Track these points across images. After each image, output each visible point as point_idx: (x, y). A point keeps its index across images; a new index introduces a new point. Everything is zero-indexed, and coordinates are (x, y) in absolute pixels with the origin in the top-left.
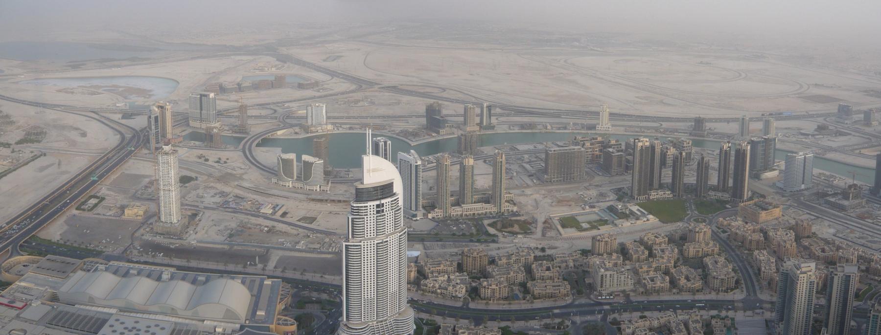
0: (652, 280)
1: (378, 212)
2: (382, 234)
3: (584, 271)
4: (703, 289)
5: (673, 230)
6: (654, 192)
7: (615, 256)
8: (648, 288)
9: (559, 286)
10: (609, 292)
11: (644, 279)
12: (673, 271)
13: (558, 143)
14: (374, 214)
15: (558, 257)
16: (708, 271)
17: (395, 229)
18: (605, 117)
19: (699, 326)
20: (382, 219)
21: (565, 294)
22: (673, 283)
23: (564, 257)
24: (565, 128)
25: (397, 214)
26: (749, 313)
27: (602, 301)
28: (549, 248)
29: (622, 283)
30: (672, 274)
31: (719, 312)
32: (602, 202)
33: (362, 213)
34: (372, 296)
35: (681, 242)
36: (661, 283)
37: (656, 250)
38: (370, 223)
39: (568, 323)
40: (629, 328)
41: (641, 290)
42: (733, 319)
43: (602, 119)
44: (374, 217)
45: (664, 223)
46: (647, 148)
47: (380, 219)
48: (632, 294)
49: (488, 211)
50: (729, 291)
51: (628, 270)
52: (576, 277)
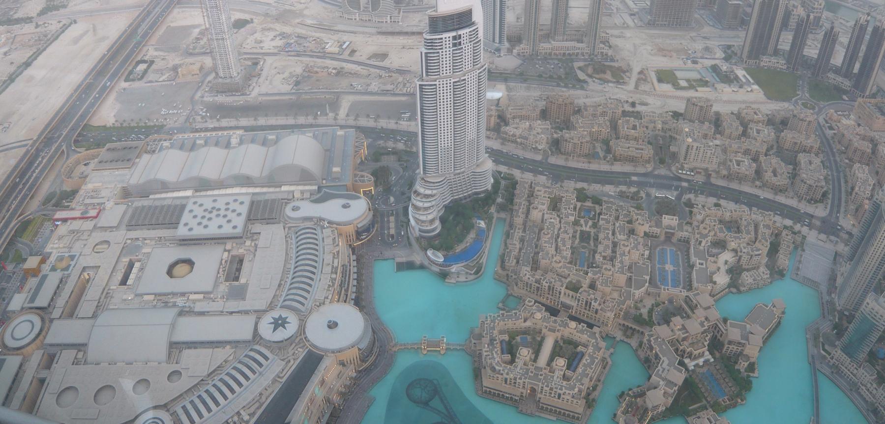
0: (738, 165)
1: (454, 45)
2: (460, 71)
3: (671, 137)
4: (786, 190)
5: (776, 110)
6: (766, 58)
8: (731, 172)
9: (642, 149)
10: (692, 167)
12: (762, 158)
14: (449, 47)
15: (647, 115)
16: (799, 171)
17: (474, 65)
20: (459, 53)
21: (646, 160)
22: (758, 173)
25: (476, 47)
26: (823, 236)
27: (682, 176)
28: (639, 104)
29: (707, 160)
30: (761, 162)
31: (793, 223)
32: (706, 58)
33: (436, 46)
35: (780, 126)
37: (751, 129)
38: (446, 70)
39: (643, 194)
41: (725, 172)
42: (804, 237)
44: (450, 51)
45: (769, 98)
47: (457, 53)
48: (714, 175)
50: (813, 202)
51: (716, 145)
52: (661, 142)
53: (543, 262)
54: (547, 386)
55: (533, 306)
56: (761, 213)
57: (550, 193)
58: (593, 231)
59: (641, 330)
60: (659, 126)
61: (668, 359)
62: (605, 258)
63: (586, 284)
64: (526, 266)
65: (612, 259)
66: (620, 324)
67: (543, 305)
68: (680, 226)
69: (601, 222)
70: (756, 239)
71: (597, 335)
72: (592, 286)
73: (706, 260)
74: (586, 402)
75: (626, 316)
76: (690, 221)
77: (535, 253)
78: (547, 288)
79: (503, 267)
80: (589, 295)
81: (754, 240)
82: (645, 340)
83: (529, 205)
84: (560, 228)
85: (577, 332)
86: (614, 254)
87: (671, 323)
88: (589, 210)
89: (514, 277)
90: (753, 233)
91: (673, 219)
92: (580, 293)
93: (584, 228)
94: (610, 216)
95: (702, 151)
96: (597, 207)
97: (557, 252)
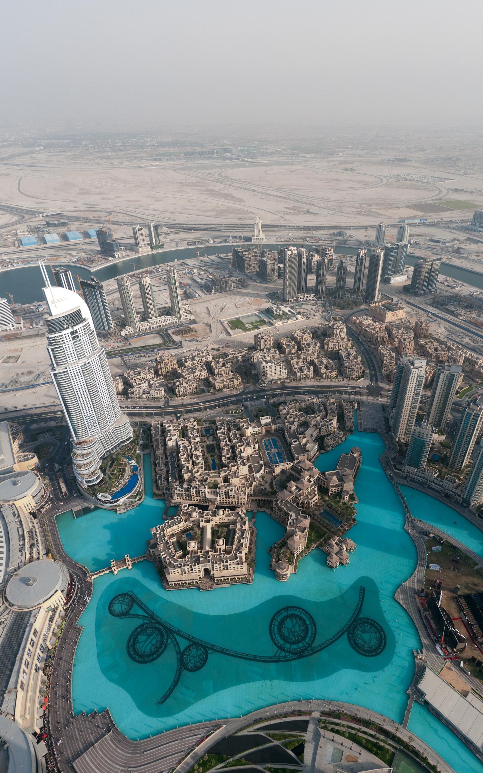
7: (272, 350)
9: (233, 378)
11: (295, 368)
12: (316, 361)
13: (221, 256)
18: (260, 228)
19: (334, 407)
23: (234, 354)
24: (226, 241)
27: (265, 388)
30: (315, 363)
34: (91, 412)
36: (307, 372)
37: (303, 344)
40: (285, 409)
43: (257, 231)
46: (294, 255)
49: (171, 322)
53: (186, 476)
54: (216, 563)
55: (188, 509)
56: (325, 396)
57: (179, 426)
58: (215, 443)
59: (269, 499)
60: (240, 358)
61: (294, 512)
62: (228, 458)
63: (220, 480)
64: (175, 482)
65: (234, 458)
66: (253, 500)
67: (195, 505)
68: (274, 422)
69: (219, 435)
70: (327, 414)
71: (240, 513)
72: (226, 480)
73: (298, 438)
74: (248, 564)
75: (255, 493)
76: (279, 416)
77: (179, 471)
78: (194, 492)
79: (158, 488)
80: (226, 488)
81: (325, 414)
82: (274, 506)
83: (165, 438)
84: (192, 448)
85: (225, 516)
86: (234, 454)
87: (288, 487)
88: (207, 430)
89: (168, 493)
90: (323, 410)
91: (267, 418)
92: (219, 488)
93: (208, 443)
94: (224, 429)
95: (274, 366)
96: (213, 425)
97: (194, 466)
